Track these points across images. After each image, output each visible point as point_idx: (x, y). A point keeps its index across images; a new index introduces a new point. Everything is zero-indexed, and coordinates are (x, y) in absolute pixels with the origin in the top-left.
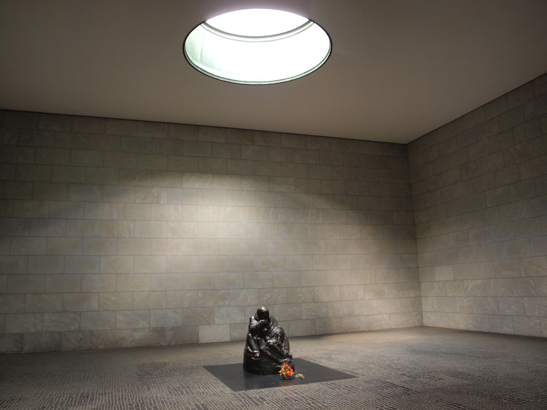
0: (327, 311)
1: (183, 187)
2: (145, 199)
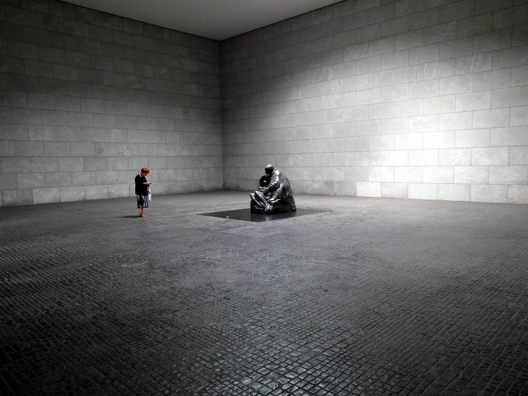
0: (488, 177)
1: (345, 61)
2: (318, 79)
